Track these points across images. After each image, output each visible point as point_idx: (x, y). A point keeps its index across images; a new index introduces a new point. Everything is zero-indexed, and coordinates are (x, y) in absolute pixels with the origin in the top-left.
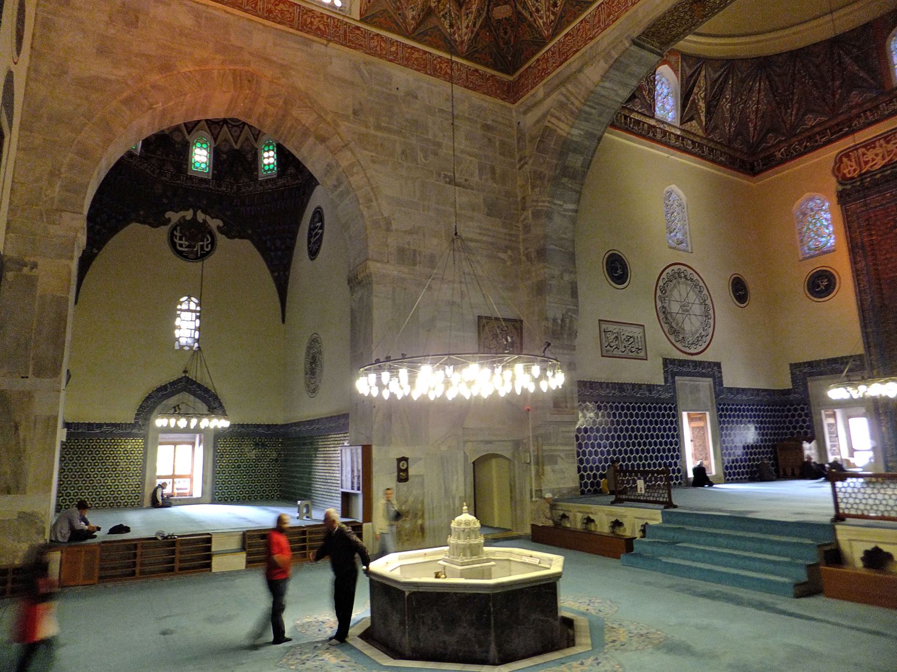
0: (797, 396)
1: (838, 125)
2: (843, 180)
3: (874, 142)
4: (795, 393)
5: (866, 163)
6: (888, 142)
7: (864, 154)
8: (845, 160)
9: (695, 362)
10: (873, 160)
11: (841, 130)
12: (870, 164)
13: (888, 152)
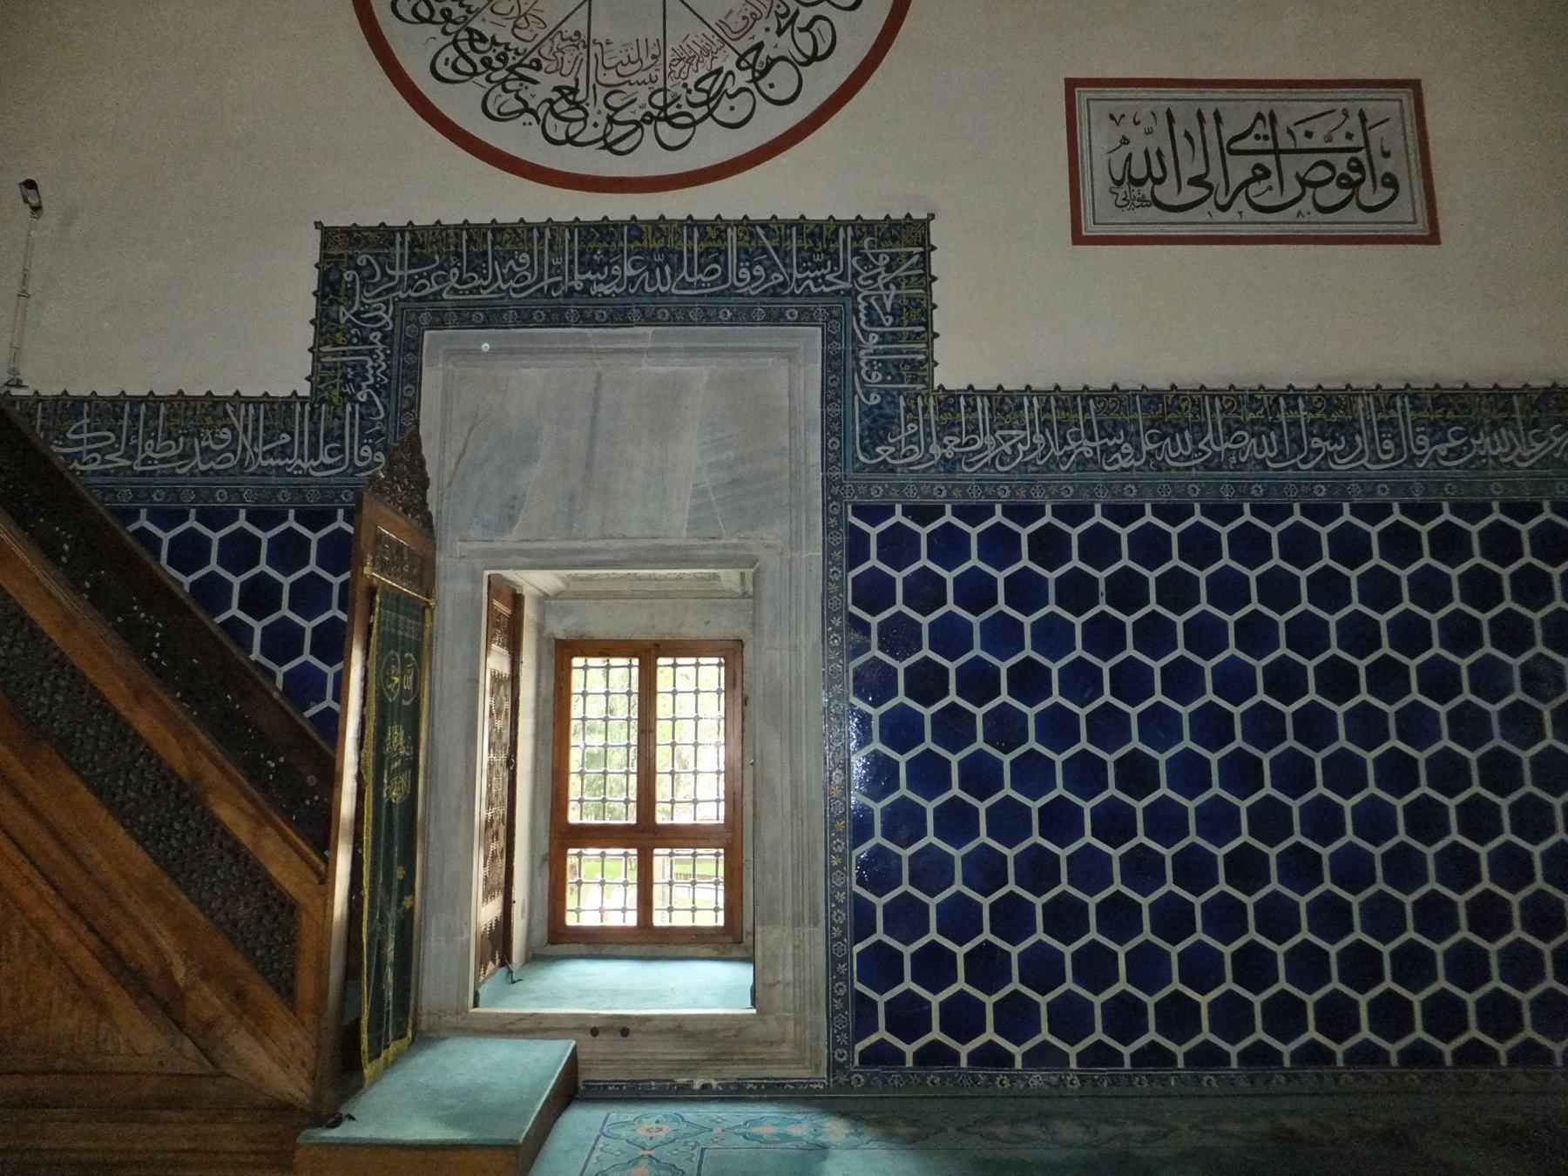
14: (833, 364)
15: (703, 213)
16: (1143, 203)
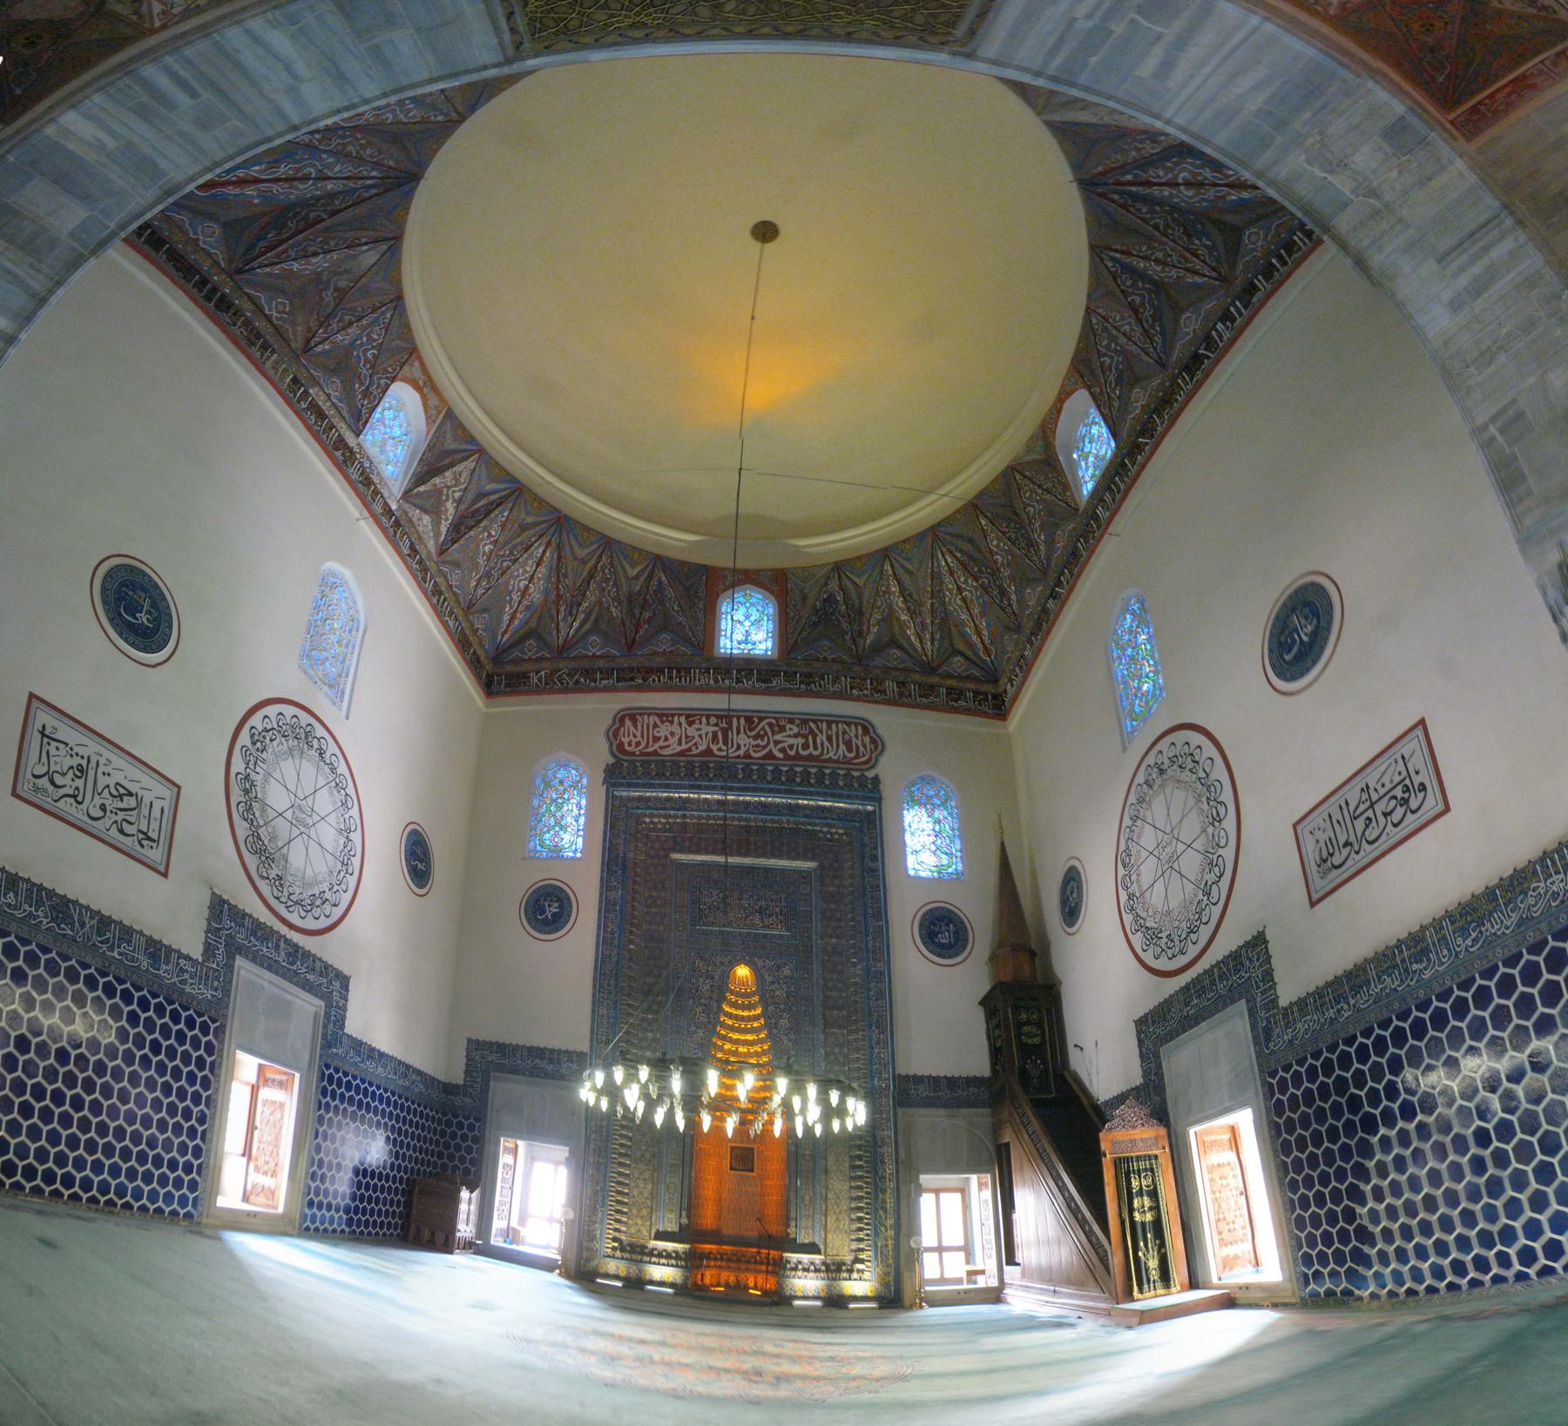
0: (468, 1100)
1: (631, 669)
2: (618, 749)
4: (465, 1094)
5: (656, 739)
6: (690, 724)
7: (655, 726)
8: (628, 723)
9: (296, 947)
10: (666, 739)
11: (632, 679)
12: (661, 743)
14: (1252, 1012)
15: (1207, 967)
16: (1330, 870)
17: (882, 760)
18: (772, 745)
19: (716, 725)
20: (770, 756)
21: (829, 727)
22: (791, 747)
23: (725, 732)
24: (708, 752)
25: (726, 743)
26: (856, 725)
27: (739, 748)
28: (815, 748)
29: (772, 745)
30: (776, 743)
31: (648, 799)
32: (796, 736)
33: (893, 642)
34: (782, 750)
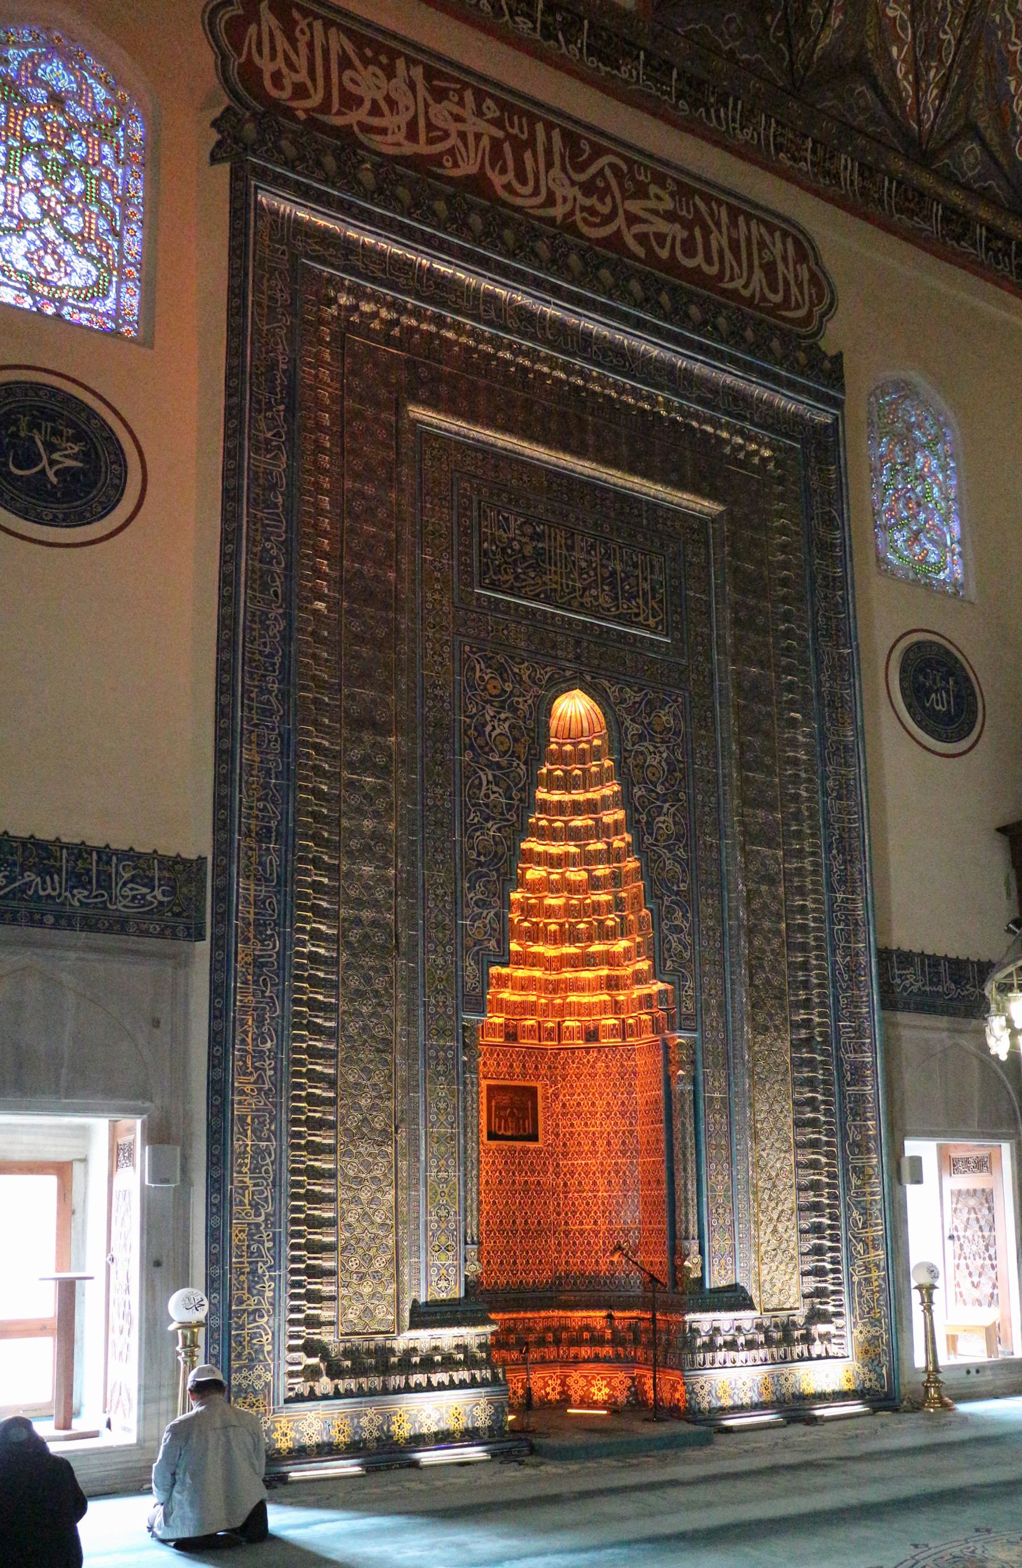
3: (393, 55)
5: (351, 101)
6: (440, 95)
7: (345, 63)
10: (375, 110)
13: (430, 126)
17: (832, 327)
18: (620, 221)
19: (497, 123)
20: (615, 242)
21: (734, 224)
22: (661, 238)
23: (519, 147)
24: (478, 183)
25: (521, 176)
26: (785, 234)
27: (551, 201)
28: (709, 261)
29: (620, 221)
30: (632, 219)
31: (350, 247)
32: (670, 216)
33: (861, 68)
34: (642, 239)
